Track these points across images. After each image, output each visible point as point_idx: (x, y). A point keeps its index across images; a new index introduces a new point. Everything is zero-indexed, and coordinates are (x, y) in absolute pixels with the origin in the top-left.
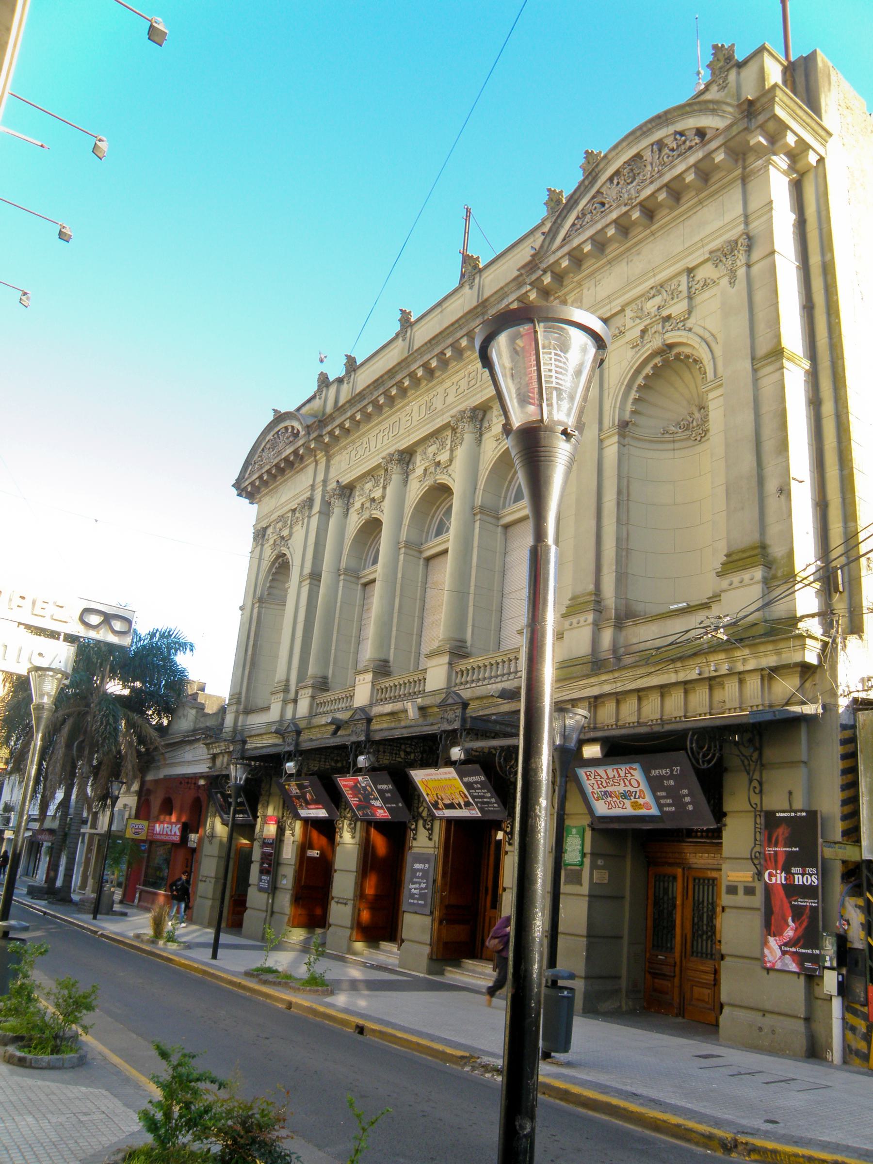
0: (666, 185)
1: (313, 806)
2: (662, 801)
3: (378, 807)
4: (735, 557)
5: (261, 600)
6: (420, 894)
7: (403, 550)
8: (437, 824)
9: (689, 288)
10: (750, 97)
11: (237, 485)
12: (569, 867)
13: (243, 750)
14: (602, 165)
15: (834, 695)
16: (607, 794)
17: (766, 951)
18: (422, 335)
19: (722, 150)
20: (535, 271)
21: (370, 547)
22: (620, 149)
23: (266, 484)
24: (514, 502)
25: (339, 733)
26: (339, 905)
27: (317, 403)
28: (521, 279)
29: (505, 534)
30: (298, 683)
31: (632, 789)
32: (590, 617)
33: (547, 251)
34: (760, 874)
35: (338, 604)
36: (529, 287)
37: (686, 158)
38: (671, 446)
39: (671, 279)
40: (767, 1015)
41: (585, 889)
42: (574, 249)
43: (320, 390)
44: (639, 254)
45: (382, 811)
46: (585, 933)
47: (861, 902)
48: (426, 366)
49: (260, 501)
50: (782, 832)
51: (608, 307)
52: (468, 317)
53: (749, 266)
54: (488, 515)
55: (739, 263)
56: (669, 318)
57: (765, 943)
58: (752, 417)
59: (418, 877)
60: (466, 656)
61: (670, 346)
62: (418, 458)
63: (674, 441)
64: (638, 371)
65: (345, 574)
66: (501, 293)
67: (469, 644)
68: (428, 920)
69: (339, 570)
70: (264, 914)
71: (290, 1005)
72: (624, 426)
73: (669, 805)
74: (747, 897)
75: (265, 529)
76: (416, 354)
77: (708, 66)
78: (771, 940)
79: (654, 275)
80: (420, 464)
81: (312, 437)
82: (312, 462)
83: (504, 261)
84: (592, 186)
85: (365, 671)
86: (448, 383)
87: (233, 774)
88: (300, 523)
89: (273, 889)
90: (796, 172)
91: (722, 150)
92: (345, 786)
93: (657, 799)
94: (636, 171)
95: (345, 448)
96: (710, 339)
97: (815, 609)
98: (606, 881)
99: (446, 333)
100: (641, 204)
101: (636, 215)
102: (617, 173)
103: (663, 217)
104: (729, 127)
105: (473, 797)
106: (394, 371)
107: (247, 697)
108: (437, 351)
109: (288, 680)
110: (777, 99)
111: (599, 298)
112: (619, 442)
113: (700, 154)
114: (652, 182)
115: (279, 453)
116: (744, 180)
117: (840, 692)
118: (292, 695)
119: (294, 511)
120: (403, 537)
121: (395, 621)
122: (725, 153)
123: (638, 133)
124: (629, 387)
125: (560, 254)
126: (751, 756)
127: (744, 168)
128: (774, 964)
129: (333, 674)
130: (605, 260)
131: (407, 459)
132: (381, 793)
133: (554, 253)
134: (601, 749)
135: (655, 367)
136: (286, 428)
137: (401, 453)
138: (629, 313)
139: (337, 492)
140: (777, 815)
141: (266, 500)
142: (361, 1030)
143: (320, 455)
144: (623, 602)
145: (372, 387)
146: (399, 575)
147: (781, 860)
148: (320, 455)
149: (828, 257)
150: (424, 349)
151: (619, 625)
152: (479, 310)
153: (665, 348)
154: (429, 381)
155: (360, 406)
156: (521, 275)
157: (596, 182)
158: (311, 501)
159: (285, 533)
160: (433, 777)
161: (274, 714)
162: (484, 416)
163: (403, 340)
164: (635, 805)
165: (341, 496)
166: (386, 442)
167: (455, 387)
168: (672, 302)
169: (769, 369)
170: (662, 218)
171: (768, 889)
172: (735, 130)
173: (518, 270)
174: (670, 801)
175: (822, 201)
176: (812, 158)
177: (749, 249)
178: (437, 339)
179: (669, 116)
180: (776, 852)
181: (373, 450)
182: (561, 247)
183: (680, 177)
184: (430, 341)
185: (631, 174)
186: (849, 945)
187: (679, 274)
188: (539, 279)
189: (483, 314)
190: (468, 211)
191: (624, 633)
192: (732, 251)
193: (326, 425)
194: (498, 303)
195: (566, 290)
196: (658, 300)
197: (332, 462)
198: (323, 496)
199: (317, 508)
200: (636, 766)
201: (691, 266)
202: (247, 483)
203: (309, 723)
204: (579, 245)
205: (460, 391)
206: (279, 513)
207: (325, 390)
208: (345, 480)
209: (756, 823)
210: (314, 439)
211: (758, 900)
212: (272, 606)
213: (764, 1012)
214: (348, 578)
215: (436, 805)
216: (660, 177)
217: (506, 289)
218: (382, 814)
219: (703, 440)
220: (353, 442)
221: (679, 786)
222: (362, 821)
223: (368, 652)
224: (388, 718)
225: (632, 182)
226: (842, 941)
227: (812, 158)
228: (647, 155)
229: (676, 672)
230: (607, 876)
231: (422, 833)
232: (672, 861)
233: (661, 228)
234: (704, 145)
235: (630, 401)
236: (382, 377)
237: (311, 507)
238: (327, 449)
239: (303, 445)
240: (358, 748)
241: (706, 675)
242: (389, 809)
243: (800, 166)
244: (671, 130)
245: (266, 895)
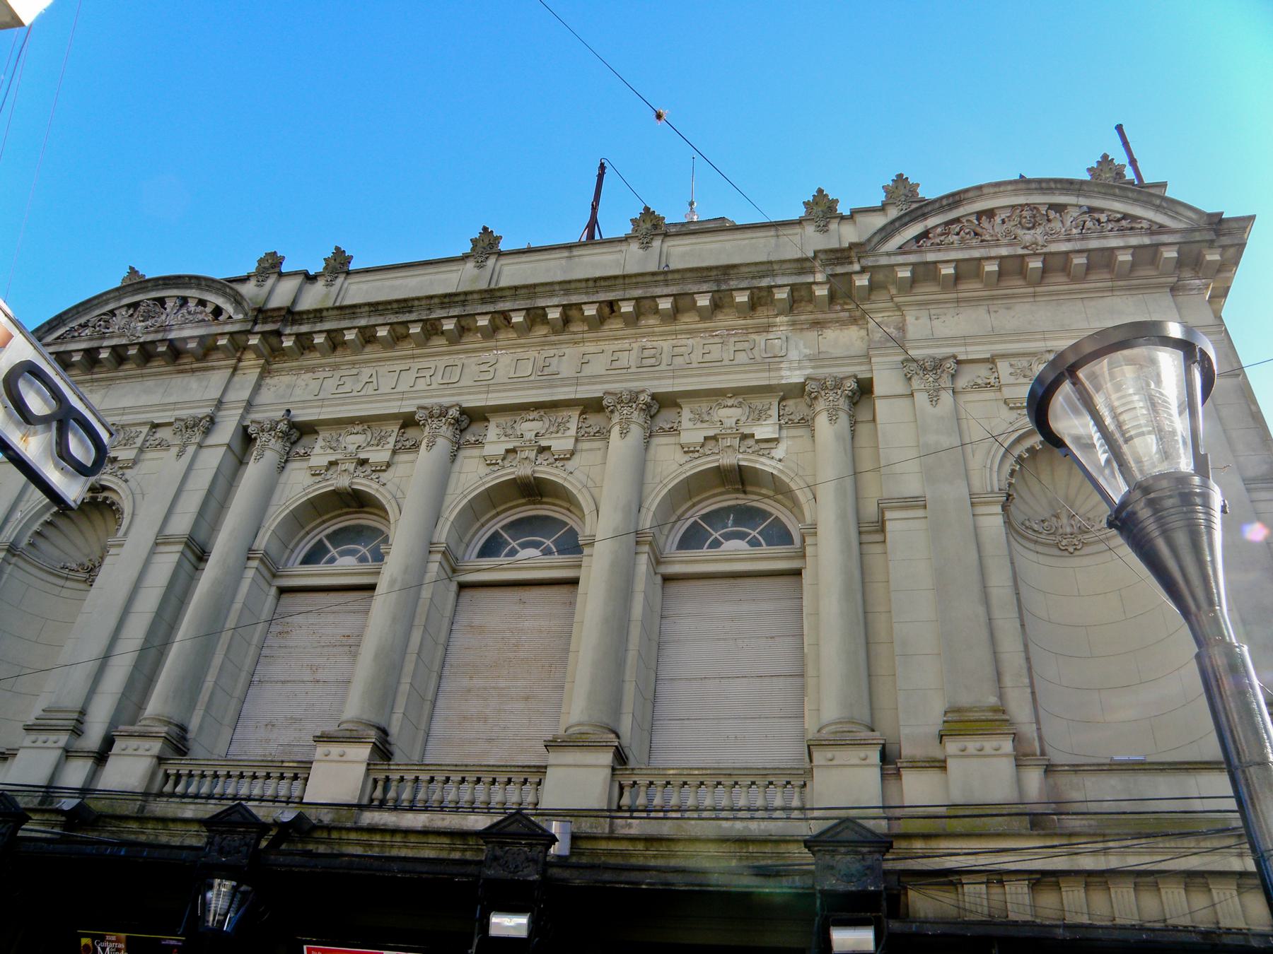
14: (971, 194)
20: (842, 264)
21: (308, 533)
22: (1002, 189)
35: (237, 605)
44: (1008, 308)
51: (963, 349)
52: (689, 275)
65: (261, 560)
76: (557, 288)
80: (494, 439)
81: (258, 328)
82: (227, 367)
83: (694, 241)
84: (951, 209)
85: (352, 738)
86: (590, 347)
88: (174, 450)
95: (312, 369)
106: (499, 294)
113: (1146, 240)
119: (155, 426)
121: (409, 667)
123: (1033, 186)
125: (900, 259)
129: (201, 727)
137: (463, 411)
143: (251, 364)
145: (436, 301)
148: (251, 364)
150: (578, 285)
152: (714, 273)
157: (956, 207)
162: (299, 439)
165: (285, 435)
170: (1056, 284)
178: (612, 282)
184: (596, 280)
190: (602, 167)
193: (294, 323)
194: (753, 278)
195: (873, 306)
197: (268, 381)
203: (142, 808)
204: (935, 263)
205: (616, 365)
208: (302, 415)
210: (263, 333)
216: (1083, 239)
217: (776, 267)
219: (1077, 553)
220: (336, 367)
224: (446, 840)
233: (1050, 294)
237: (207, 432)
238: (273, 353)
244: (1083, 201)
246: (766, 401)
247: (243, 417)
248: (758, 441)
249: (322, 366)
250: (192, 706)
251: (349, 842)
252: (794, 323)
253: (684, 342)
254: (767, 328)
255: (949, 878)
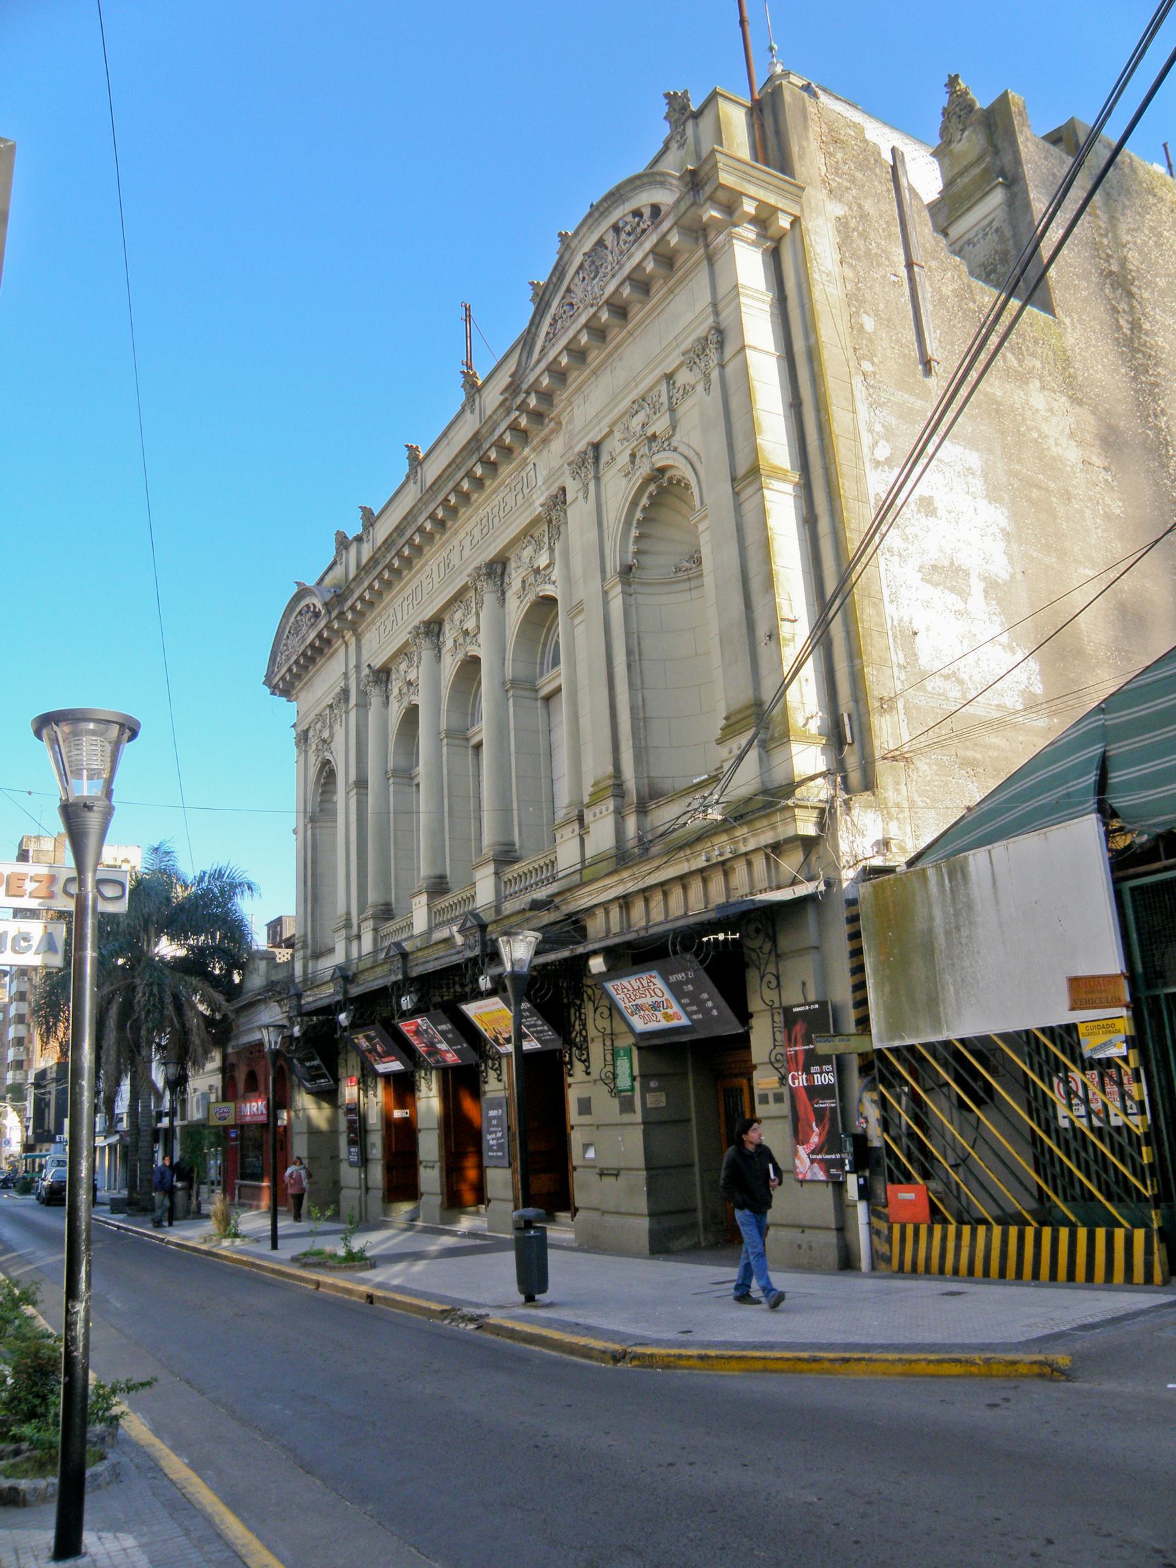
0: (628, 277)
2: (689, 1009)
4: (733, 720)
5: (313, 820)
6: (498, 1145)
7: (445, 741)
9: (670, 398)
10: (690, 167)
11: (268, 681)
13: (300, 1006)
15: (837, 869)
16: (639, 1008)
17: (797, 1162)
18: (432, 471)
19: (675, 230)
22: (581, 234)
23: (298, 677)
24: (553, 667)
27: (339, 570)
28: (508, 404)
29: (547, 707)
30: (359, 915)
31: (659, 1000)
32: (610, 804)
33: (526, 368)
34: (783, 1079)
36: (517, 413)
37: (641, 244)
38: (686, 586)
39: (651, 389)
40: (807, 1231)
41: (638, 1117)
42: (551, 363)
43: (339, 552)
46: (642, 1165)
47: (875, 1096)
48: (432, 517)
49: (297, 698)
50: (799, 1029)
52: (464, 454)
53: (722, 366)
54: (522, 689)
55: (712, 365)
56: (654, 437)
57: (795, 1153)
58: (736, 552)
59: (494, 1126)
60: (516, 860)
61: (662, 470)
62: (447, 627)
63: (689, 579)
64: (634, 503)
66: (490, 423)
67: (517, 847)
68: (508, 1172)
69: (387, 772)
70: (358, 1193)
71: (318, 1284)
72: (627, 571)
73: (695, 1013)
74: (777, 1105)
75: (306, 732)
77: (665, 118)
78: (800, 1148)
79: (637, 385)
80: (450, 635)
84: (561, 282)
85: (420, 893)
86: (462, 534)
87: (267, 1039)
89: (364, 1161)
90: (771, 239)
91: (675, 230)
92: (409, 1031)
93: (683, 1007)
94: (598, 263)
95: (373, 623)
96: (694, 459)
97: (822, 767)
98: (663, 1105)
99: (445, 476)
100: (607, 302)
101: (605, 316)
102: (581, 267)
103: (637, 313)
104: (678, 201)
107: (313, 938)
108: (440, 498)
109: (348, 913)
110: (720, 165)
111: (589, 418)
112: (623, 592)
113: (653, 239)
114: (613, 276)
115: (304, 639)
116: (710, 259)
117: (843, 862)
118: (355, 931)
119: (331, 706)
120: (443, 726)
122: (679, 233)
124: (628, 523)
125: (538, 370)
126: (761, 948)
127: (707, 246)
128: (805, 1175)
130: (588, 371)
131: (436, 630)
132: (442, 1033)
133: (532, 370)
134: (606, 961)
135: (651, 496)
136: (308, 606)
138: (617, 435)
139: (371, 679)
140: (795, 1010)
141: (303, 695)
142: (370, 1298)
144: (646, 781)
146: (445, 772)
147: (801, 1058)
148: (348, 635)
149: (812, 340)
151: (642, 810)
153: (655, 473)
154: (443, 534)
155: (375, 573)
156: (506, 400)
158: (345, 692)
159: (326, 735)
161: (338, 958)
163: (415, 483)
164: (667, 1017)
165: (377, 682)
166: (411, 612)
167: (469, 538)
168: (655, 417)
169: (750, 491)
170: (636, 314)
171: (793, 1092)
172: (683, 207)
173: (501, 394)
174: (695, 1008)
175: (802, 270)
176: (784, 222)
177: (721, 345)
179: (622, 192)
180: (796, 1052)
181: (400, 623)
182: (539, 361)
183: (639, 266)
185: (593, 268)
186: (869, 1144)
187: (658, 382)
188: (524, 401)
189: (478, 449)
190: (468, 309)
191: (649, 818)
192: (704, 350)
193: (346, 599)
196: (641, 417)
197: (363, 642)
198: (358, 685)
199: (353, 700)
200: (654, 973)
201: (668, 371)
202: (277, 678)
206: (317, 711)
207: (344, 552)
208: (377, 663)
209: (773, 1021)
210: (336, 618)
211: (785, 1108)
212: (326, 825)
213: (803, 1228)
214: (401, 781)
216: (620, 268)
218: (451, 1058)
220: (380, 614)
221: (699, 989)
222: (437, 1068)
223: (424, 870)
225: (595, 277)
226: (861, 1140)
227: (784, 222)
228: (610, 239)
229: (688, 860)
230: (663, 1098)
231: (492, 1075)
232: (737, 1071)
233: (638, 326)
234: (657, 227)
235: (632, 540)
236: (390, 535)
237: (347, 700)
238: (354, 627)
239: (326, 626)
240: (399, 988)
241: (714, 861)
242: (457, 1052)
243: (772, 231)
245: (357, 1170)
246: (540, 531)
247: (357, 678)
248: (545, 569)
249: (375, 618)
250: (389, 891)
252: (534, 449)
253: (492, 505)
254: (525, 462)
255: (590, 910)
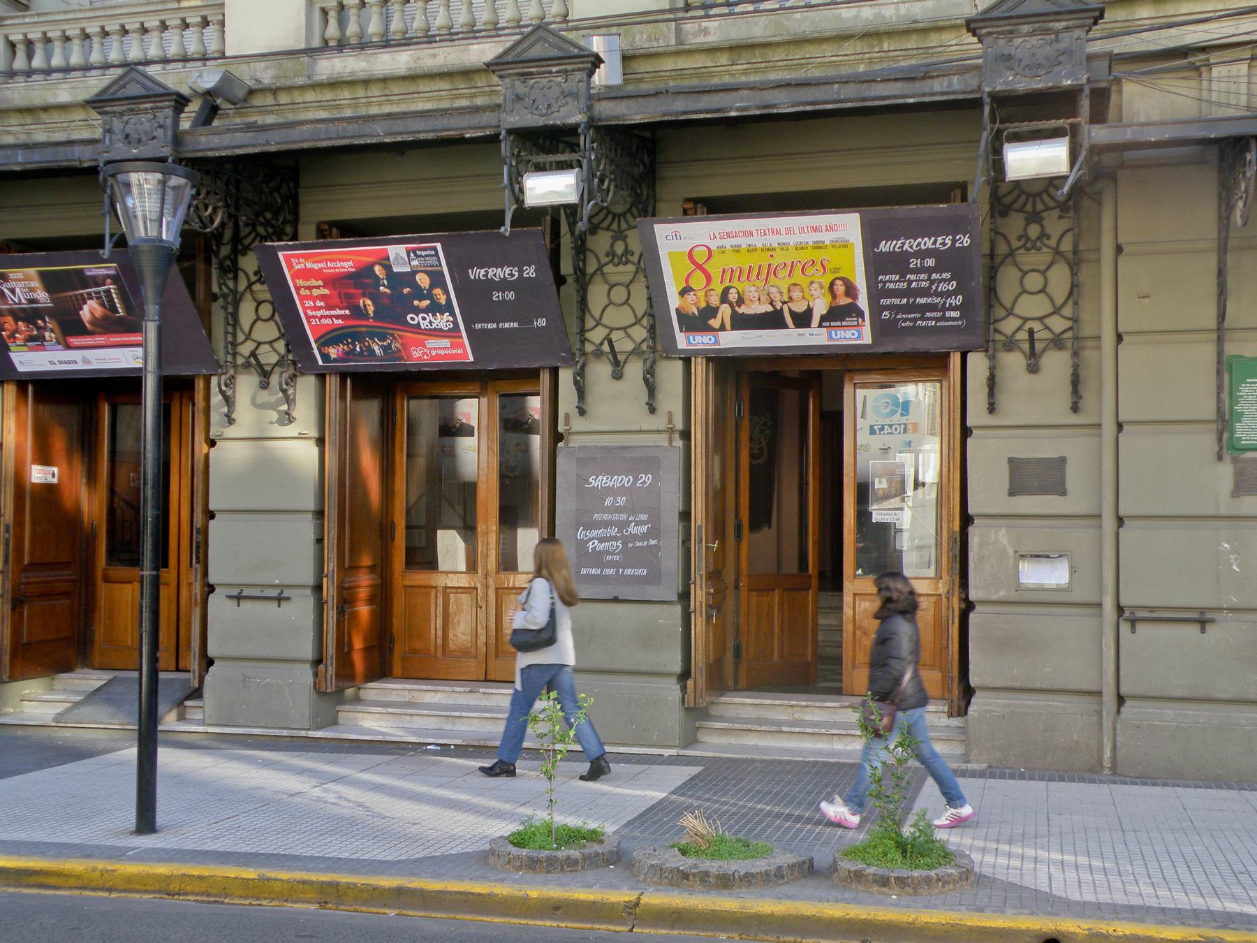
1: (100, 340)
3: (437, 333)
8: (671, 373)
12: (1248, 455)
25: (216, 123)
26: (247, 605)
45: (446, 343)
59: (619, 510)
92: (297, 275)
105: (876, 293)
160: (743, 242)
215: (698, 322)
224: (445, 85)
251: (307, 106)
